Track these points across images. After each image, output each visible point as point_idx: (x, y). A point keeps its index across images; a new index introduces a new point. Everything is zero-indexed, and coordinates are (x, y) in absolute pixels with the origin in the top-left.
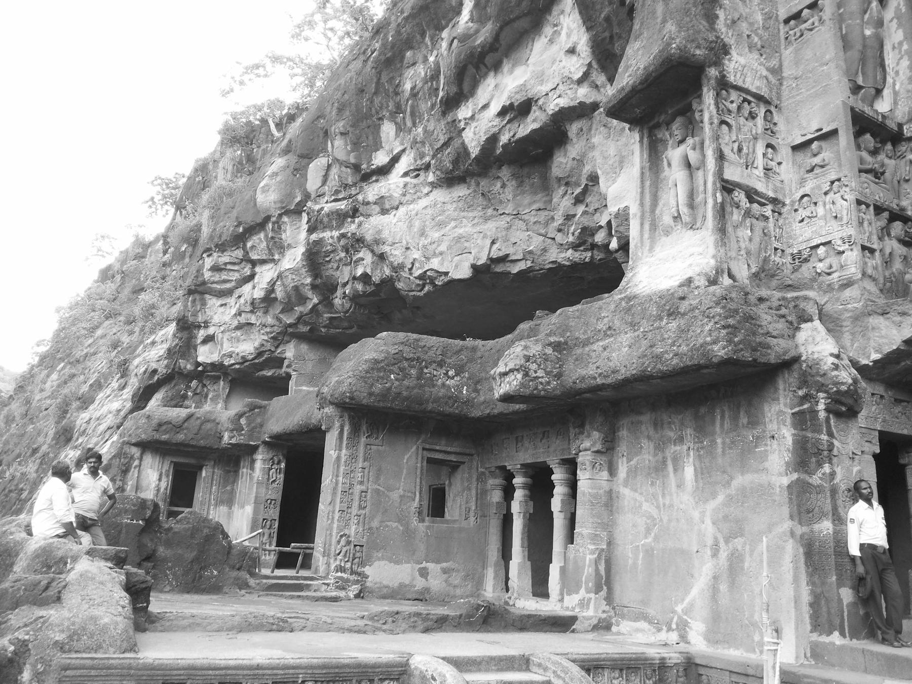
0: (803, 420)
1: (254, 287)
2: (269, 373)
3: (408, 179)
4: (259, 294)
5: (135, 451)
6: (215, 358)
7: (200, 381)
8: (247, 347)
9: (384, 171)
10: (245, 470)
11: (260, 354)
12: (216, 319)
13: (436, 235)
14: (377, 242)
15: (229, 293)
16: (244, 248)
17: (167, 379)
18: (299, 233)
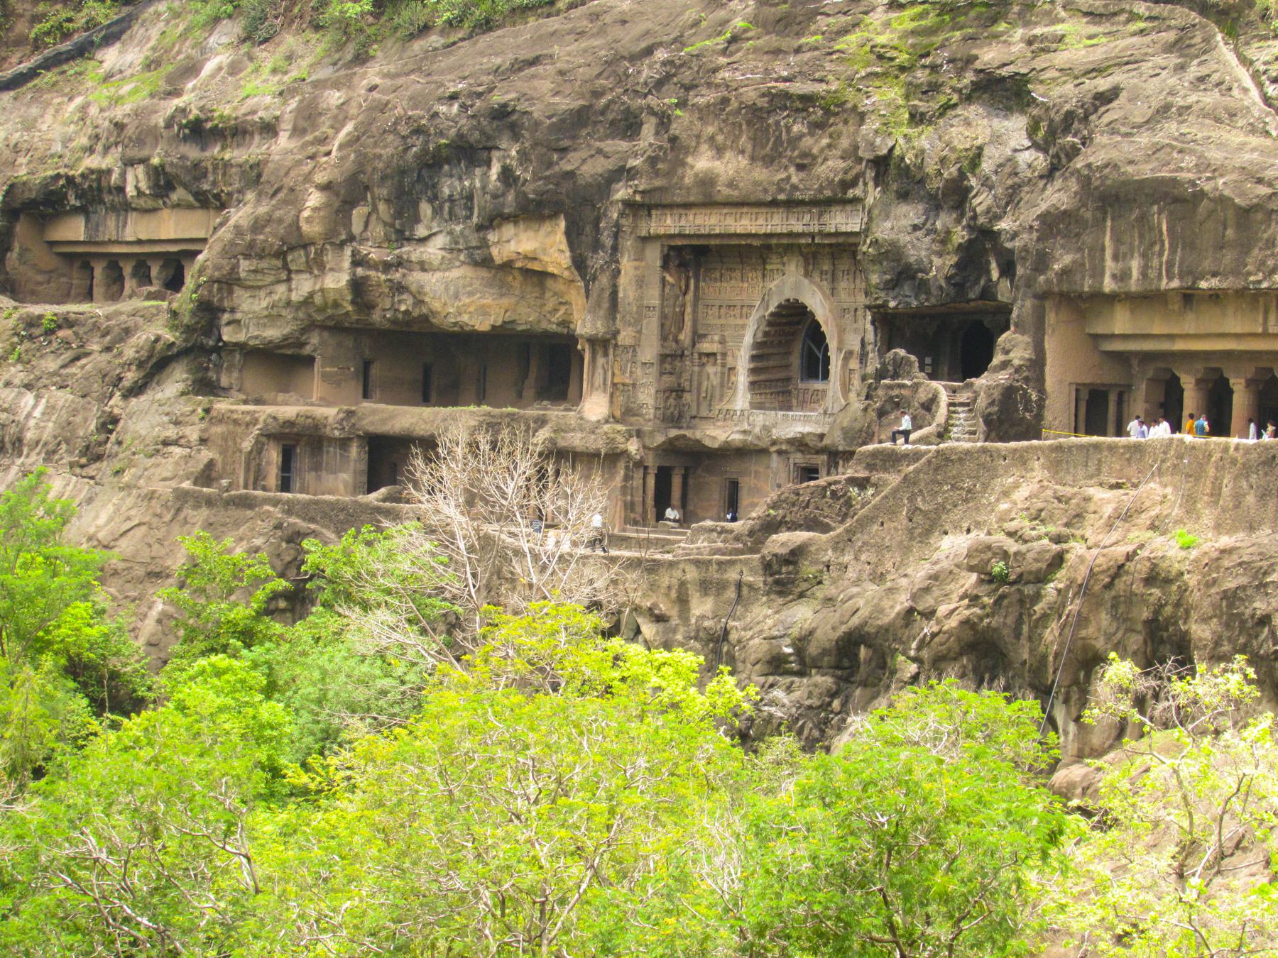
0: (627, 468)
1: (290, 290)
2: (289, 352)
3: (443, 253)
4: (295, 297)
5: (264, 439)
6: (241, 337)
7: (219, 355)
8: (273, 333)
9: (423, 240)
10: (332, 449)
11: (286, 338)
12: (245, 307)
13: (467, 301)
14: (419, 293)
15: (260, 288)
16: (285, 259)
17: (184, 353)
18: (342, 261)
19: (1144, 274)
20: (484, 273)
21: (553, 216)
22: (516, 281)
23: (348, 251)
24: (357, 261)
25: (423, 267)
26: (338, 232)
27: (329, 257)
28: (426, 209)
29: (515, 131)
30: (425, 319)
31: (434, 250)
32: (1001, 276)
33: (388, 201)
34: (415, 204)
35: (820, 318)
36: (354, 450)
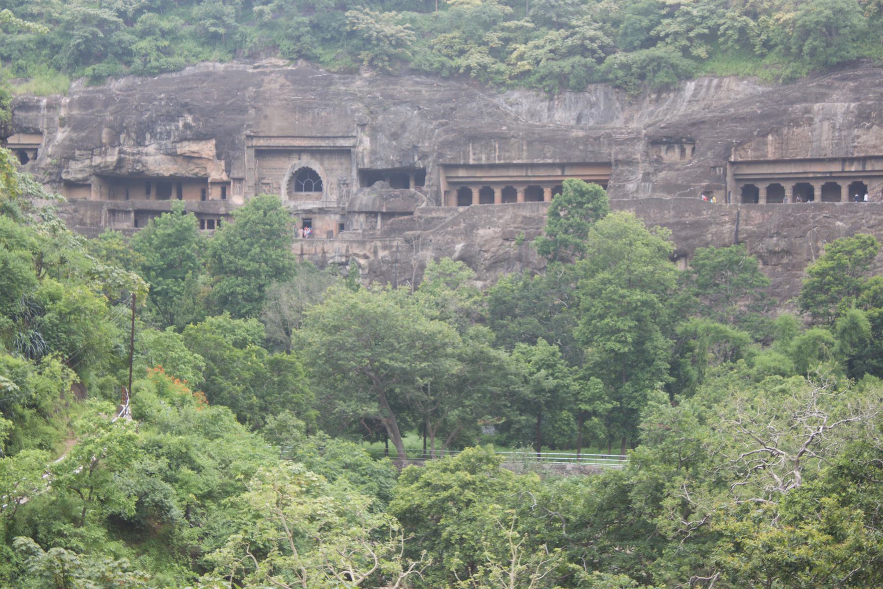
4: (93, 164)
6: (69, 177)
8: (80, 176)
9: (147, 146)
19: (488, 159)
20: (169, 157)
21: (210, 139)
22: (180, 160)
23: (117, 149)
24: (120, 152)
25: (147, 154)
26: (114, 141)
27: (109, 151)
28: (148, 136)
29: (190, 112)
30: (143, 171)
31: (151, 148)
32: (419, 159)
33: (135, 132)
34: (144, 134)
35: (318, 172)
36: (132, 215)
